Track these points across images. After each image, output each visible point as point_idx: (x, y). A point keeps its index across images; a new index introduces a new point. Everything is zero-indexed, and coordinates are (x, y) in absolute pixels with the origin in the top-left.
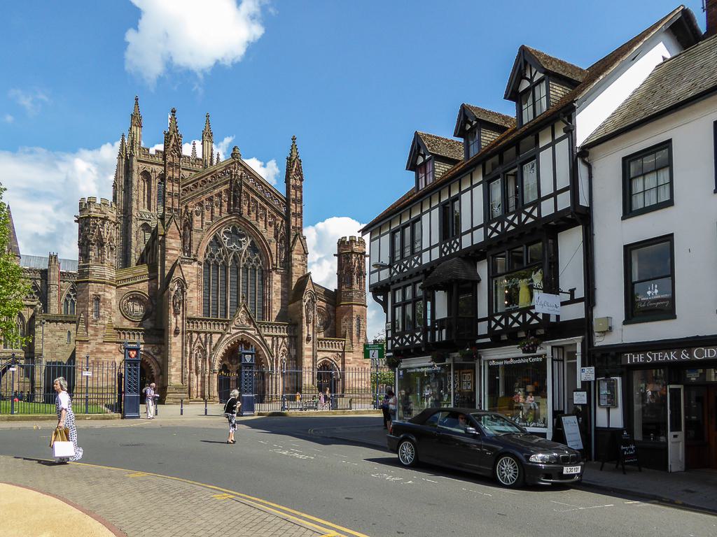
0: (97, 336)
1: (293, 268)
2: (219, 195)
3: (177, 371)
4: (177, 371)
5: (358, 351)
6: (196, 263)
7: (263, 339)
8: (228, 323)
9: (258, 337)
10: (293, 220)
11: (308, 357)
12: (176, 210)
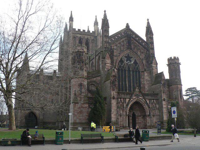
0: (81, 100)
1: (154, 70)
2: (123, 41)
3: (114, 115)
4: (114, 115)
7: (145, 100)
8: (131, 95)
10: (151, 51)
11: (165, 108)
12: (108, 48)
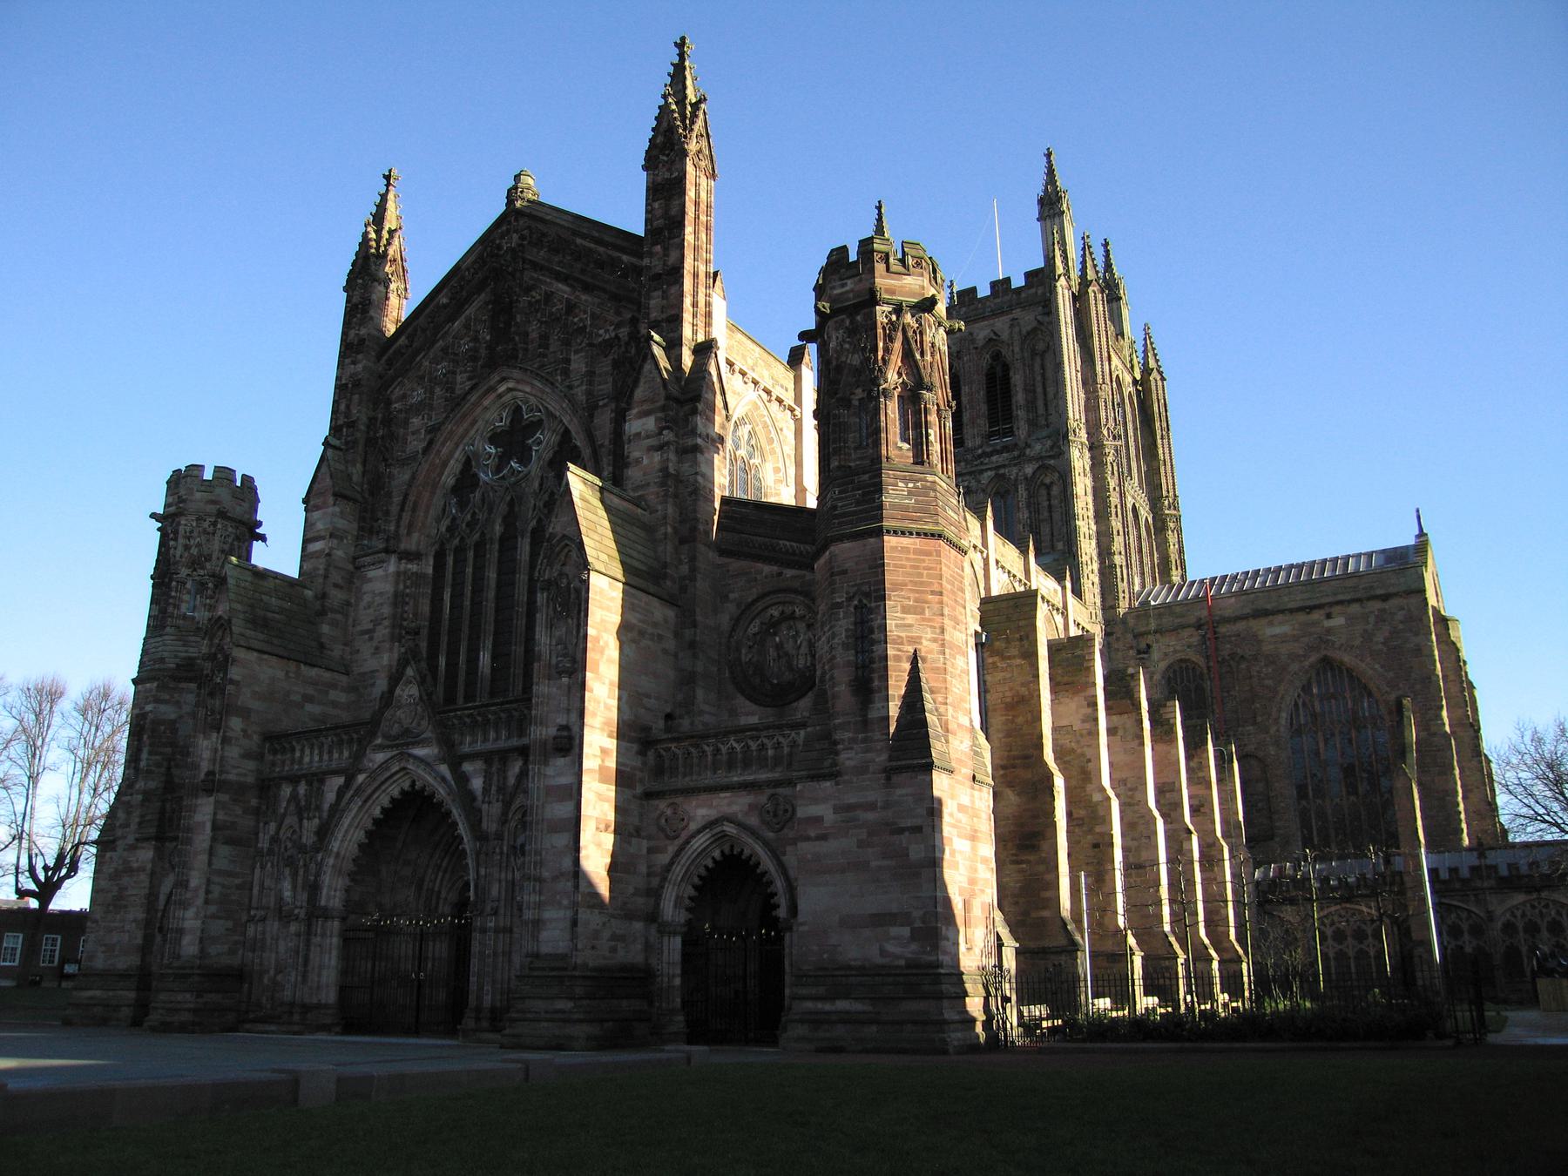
5: (862, 770)
6: (393, 559)
9: (444, 769)
